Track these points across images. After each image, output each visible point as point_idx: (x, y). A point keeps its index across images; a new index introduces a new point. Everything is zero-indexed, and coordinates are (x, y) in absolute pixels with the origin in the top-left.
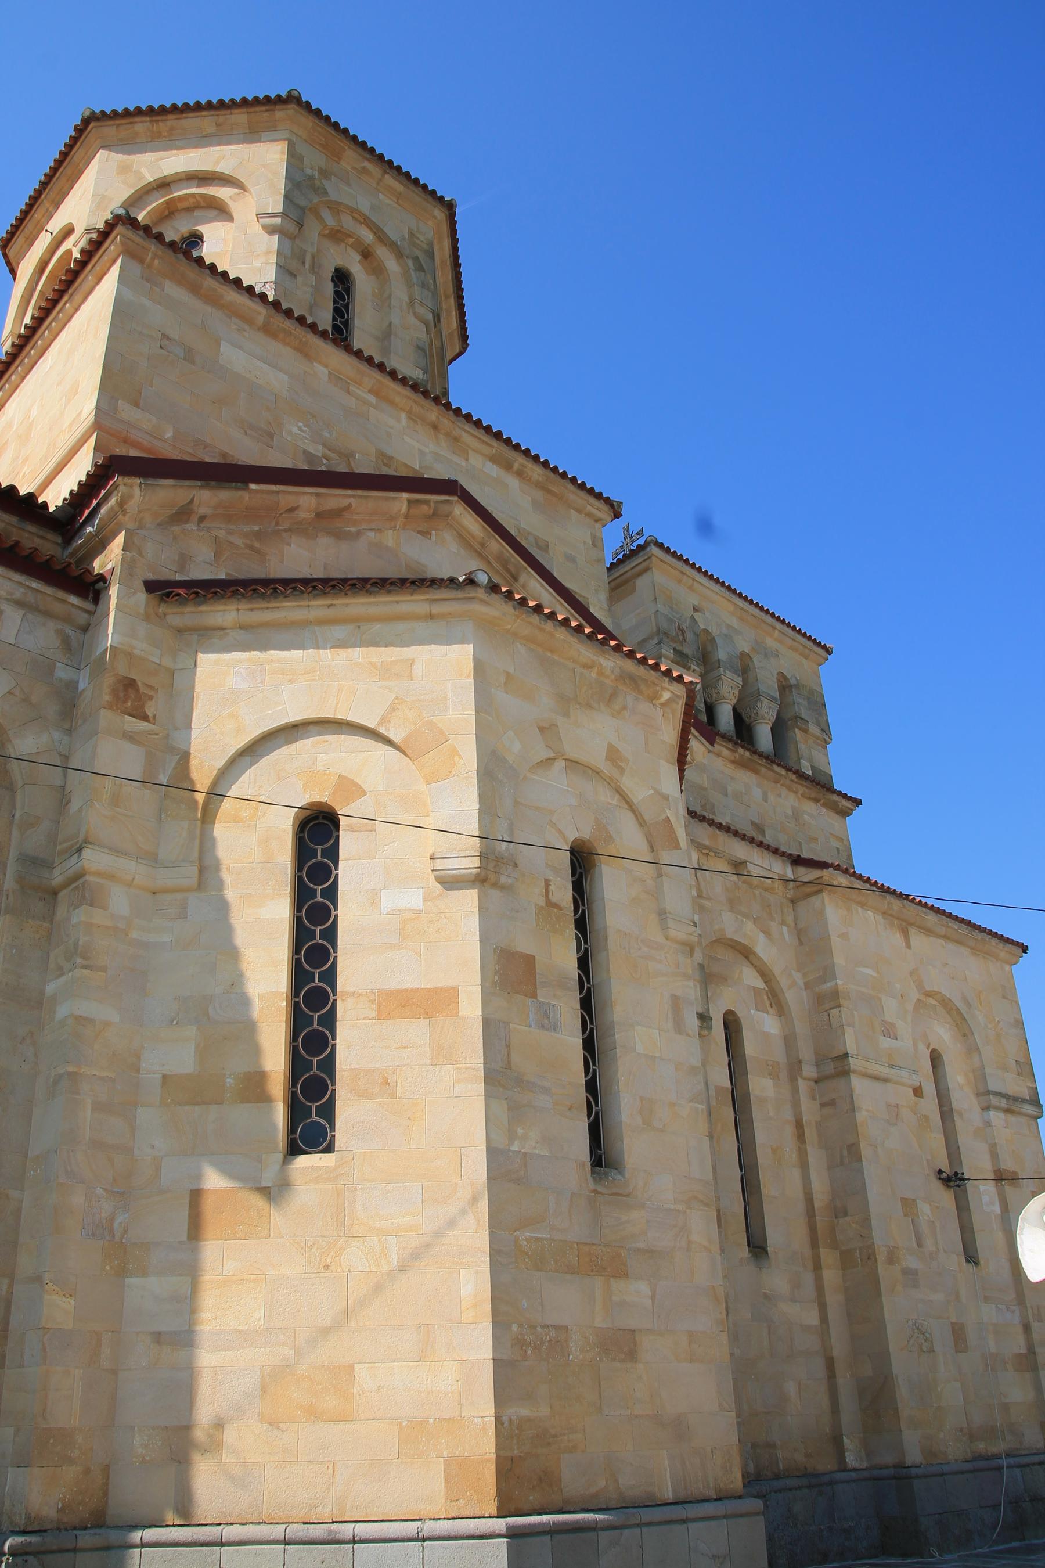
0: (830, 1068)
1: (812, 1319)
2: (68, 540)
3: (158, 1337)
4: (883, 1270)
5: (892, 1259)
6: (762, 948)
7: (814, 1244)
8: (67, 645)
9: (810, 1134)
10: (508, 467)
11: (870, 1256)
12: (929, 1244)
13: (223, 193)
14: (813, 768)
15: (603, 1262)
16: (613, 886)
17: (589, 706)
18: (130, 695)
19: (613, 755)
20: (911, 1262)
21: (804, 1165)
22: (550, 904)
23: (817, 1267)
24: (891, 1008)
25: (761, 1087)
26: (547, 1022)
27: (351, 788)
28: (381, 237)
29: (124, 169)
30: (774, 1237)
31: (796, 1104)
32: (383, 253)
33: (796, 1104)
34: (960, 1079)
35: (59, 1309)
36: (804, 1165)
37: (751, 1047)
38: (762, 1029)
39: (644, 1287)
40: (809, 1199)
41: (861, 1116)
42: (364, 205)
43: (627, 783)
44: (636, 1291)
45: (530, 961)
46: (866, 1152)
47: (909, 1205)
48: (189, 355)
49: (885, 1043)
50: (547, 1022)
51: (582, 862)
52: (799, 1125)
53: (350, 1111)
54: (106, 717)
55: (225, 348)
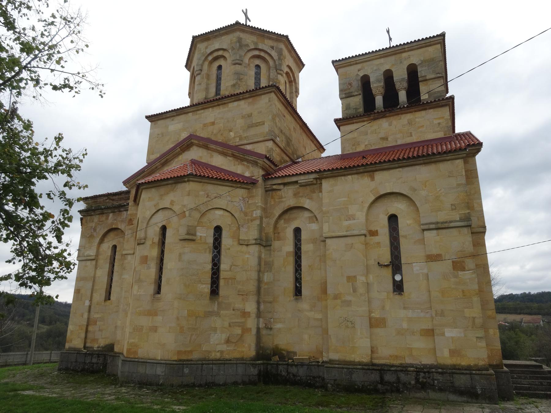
17: (168, 193)
19: (172, 203)
20: (348, 298)
22: (153, 243)
24: (353, 209)
28: (224, 50)
37: (304, 236)
39: (161, 318)
44: (159, 318)
45: (147, 257)
47: (351, 279)
49: (346, 223)
50: (149, 268)
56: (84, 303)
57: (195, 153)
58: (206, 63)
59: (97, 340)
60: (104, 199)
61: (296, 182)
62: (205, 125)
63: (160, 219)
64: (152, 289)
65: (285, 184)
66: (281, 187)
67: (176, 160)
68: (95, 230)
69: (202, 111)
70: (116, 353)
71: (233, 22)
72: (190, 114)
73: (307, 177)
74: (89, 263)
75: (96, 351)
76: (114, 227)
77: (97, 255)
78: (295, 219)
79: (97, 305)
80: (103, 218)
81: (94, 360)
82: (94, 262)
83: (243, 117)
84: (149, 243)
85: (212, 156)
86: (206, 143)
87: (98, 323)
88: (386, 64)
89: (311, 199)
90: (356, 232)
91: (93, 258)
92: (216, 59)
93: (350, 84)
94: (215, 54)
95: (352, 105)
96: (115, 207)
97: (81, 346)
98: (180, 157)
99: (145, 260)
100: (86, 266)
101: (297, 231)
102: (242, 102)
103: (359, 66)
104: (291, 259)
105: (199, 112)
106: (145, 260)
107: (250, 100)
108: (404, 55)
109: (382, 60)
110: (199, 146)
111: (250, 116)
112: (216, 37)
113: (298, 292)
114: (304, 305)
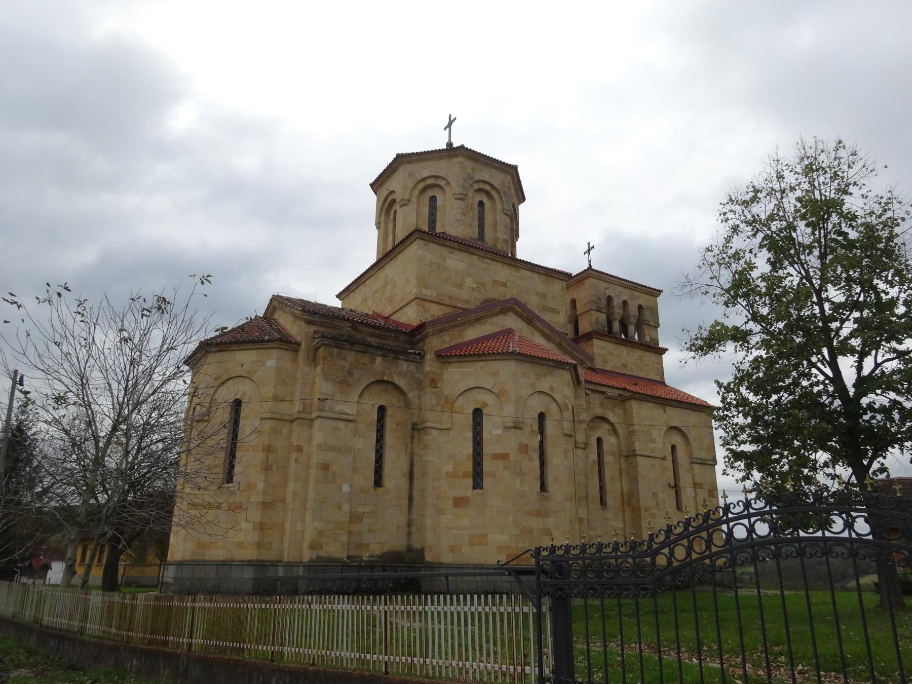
0: (631, 453)
1: (621, 525)
3: (448, 528)
4: (642, 512)
5: (647, 510)
6: (611, 417)
7: (623, 505)
8: (417, 369)
9: (624, 473)
10: (534, 271)
11: (639, 509)
12: (662, 506)
13: (442, 183)
14: (651, 339)
15: (542, 513)
16: (549, 424)
18: (434, 383)
19: (551, 388)
20: (655, 511)
21: (621, 482)
23: (624, 511)
24: (655, 434)
25: (608, 459)
26: (531, 460)
27: (485, 404)
29: (411, 174)
30: (610, 502)
31: (620, 464)
32: (493, 193)
33: (620, 464)
34: (683, 454)
35: (428, 522)
36: (621, 482)
37: (606, 447)
38: (610, 442)
40: (622, 492)
41: (639, 468)
42: (487, 178)
43: (554, 395)
44: (551, 520)
45: (527, 445)
46: (640, 478)
47: (655, 495)
48: (438, 266)
49: (651, 445)
50: (531, 460)
51: (542, 417)
52: (621, 470)
53: (486, 481)
54: (428, 390)
55: (448, 260)
56: (341, 488)
57: (510, 321)
59: (367, 546)
60: (347, 324)
61: (603, 393)
62: (495, 282)
63: (537, 404)
65: (593, 391)
66: (589, 392)
68: (350, 374)
70: (428, 563)
71: (512, 163)
72: (475, 257)
73: (614, 391)
74: (341, 425)
75: (368, 561)
76: (386, 378)
78: (598, 428)
79: (361, 491)
80: (365, 359)
81: (377, 574)
82: (351, 425)
83: (537, 294)
84: (527, 429)
85: (533, 335)
86: (530, 318)
87: (365, 520)
88: (625, 295)
89: (613, 412)
90: (657, 455)
92: (488, 194)
93: (600, 299)
94: (482, 186)
95: (600, 320)
96: (391, 351)
97: (343, 555)
99: (524, 449)
100: (336, 429)
101: (599, 440)
102: (535, 276)
103: (606, 285)
104: (596, 467)
105: (486, 260)
106: (524, 449)
107: (544, 278)
108: (636, 293)
109: (621, 289)
111: (544, 296)
112: (486, 164)
113: (603, 502)
114: (609, 515)
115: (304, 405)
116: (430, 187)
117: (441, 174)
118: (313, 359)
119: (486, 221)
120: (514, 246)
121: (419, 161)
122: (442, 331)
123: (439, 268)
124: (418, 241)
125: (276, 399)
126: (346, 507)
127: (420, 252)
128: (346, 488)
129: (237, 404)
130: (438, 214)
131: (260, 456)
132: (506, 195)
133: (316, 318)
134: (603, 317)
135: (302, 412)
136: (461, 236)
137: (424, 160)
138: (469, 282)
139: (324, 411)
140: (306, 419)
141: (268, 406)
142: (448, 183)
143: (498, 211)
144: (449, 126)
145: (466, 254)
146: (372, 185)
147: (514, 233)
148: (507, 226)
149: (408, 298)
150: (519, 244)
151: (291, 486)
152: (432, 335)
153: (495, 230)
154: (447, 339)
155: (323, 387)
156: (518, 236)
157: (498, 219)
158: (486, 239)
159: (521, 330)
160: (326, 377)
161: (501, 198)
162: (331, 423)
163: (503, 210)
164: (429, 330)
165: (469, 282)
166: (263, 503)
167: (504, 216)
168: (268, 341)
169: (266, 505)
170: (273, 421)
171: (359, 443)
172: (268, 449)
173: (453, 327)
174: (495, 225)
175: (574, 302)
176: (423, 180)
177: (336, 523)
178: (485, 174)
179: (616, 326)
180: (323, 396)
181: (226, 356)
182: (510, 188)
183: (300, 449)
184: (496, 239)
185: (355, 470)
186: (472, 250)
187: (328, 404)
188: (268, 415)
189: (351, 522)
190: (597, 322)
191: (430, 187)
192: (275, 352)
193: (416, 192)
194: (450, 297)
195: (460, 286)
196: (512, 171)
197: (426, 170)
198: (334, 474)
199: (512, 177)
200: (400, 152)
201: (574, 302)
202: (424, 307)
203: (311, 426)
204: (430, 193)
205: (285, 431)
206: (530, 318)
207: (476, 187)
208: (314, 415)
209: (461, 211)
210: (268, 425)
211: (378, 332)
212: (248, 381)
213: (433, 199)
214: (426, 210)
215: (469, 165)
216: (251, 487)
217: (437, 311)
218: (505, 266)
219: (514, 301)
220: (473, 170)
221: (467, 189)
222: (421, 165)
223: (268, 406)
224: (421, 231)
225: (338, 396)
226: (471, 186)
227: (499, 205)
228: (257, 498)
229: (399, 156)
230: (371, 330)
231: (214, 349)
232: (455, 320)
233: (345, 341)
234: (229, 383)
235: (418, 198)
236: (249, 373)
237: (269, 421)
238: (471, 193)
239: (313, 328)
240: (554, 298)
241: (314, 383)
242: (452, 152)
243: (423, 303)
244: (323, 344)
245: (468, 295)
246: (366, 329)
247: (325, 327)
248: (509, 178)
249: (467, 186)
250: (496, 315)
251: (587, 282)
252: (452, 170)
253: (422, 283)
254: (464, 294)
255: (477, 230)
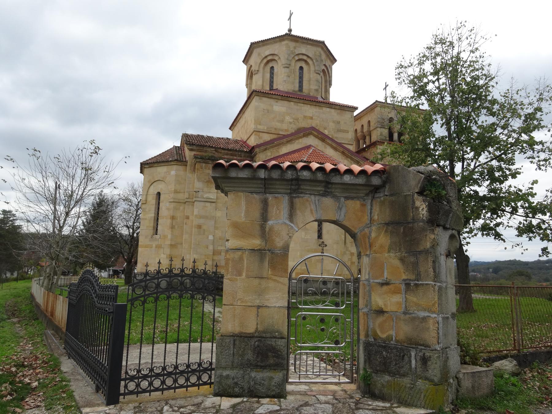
2: (252, 153)
13: (276, 58)
28: (308, 57)
29: (259, 54)
42: (304, 51)
48: (268, 111)
56: (208, 237)
58: (294, 61)
60: (212, 149)
62: (305, 117)
64: (316, 235)
67: (297, 141)
69: (302, 105)
72: (292, 103)
74: (208, 204)
77: (217, 198)
79: (220, 239)
82: (214, 204)
83: (334, 122)
85: (326, 148)
86: (323, 138)
91: (213, 201)
92: (306, 61)
95: (384, 133)
98: (300, 140)
100: (205, 207)
102: (333, 110)
105: (299, 104)
107: (339, 111)
110: (316, 137)
111: (339, 123)
115: (189, 195)
116: (269, 61)
117: (276, 53)
118: (194, 170)
119: (304, 79)
120: (327, 92)
121: (263, 45)
122: (266, 149)
123: (268, 112)
124: (256, 97)
125: (176, 192)
126: (211, 247)
127: (257, 104)
128: (211, 237)
129: (159, 194)
130: (275, 77)
131: (169, 221)
132: (317, 61)
133: (194, 147)
134: (386, 132)
135: (189, 198)
136: (286, 90)
137: (266, 45)
138: (288, 119)
139: (198, 197)
140: (189, 202)
141: (172, 195)
142: (280, 58)
143: (311, 72)
144: (290, 19)
145: (286, 102)
146: (243, 61)
147: (328, 83)
148: (317, 81)
149: (252, 131)
150: (332, 90)
151: (185, 237)
152: (260, 152)
153: (310, 84)
154: (269, 154)
155: (198, 185)
156: (330, 84)
157: (311, 76)
158: (304, 90)
159: (317, 146)
160: (199, 180)
161: (314, 63)
162: (203, 204)
163: (315, 71)
164: (257, 150)
165: (288, 119)
166: (171, 245)
167: (315, 74)
168: (171, 161)
169: (172, 246)
170: (175, 204)
171: (219, 214)
172: (173, 218)
173: (273, 147)
174: (309, 81)
175: (369, 122)
176: (266, 57)
177: (205, 255)
178: (303, 49)
179: (396, 136)
180: (197, 190)
181: (152, 170)
182: (320, 56)
183: (188, 218)
184: (310, 90)
185: (216, 228)
186: (290, 99)
187: (200, 194)
188: (172, 200)
189: (213, 254)
190: (381, 134)
191: (269, 61)
192: (175, 167)
193: (262, 65)
194: (275, 129)
195: (282, 121)
196: (321, 44)
197: (267, 51)
198: (204, 230)
199: (322, 48)
200: (253, 41)
201: (369, 122)
202: (259, 136)
203: (193, 205)
204: (271, 65)
205: (181, 208)
206: (323, 138)
207: (297, 58)
208: (194, 199)
209: (286, 74)
210: (173, 205)
211: (229, 152)
212: (163, 182)
213: (272, 68)
214: (268, 75)
215: (292, 44)
216: (165, 237)
217: (267, 138)
218: (312, 107)
219: (313, 128)
220: (295, 48)
221: (291, 61)
222: (265, 47)
223: (172, 195)
224: (256, 91)
225: (206, 189)
226: (293, 58)
227: (312, 68)
228: (168, 242)
229: (252, 44)
230: (226, 151)
231: (147, 166)
232: (273, 143)
233: (209, 159)
234: (155, 184)
235: (264, 68)
236: (163, 178)
237: (173, 203)
238: (293, 63)
239: (193, 153)
240: (345, 123)
241: (194, 183)
242: (289, 37)
243: (258, 133)
244: (197, 162)
245: (287, 126)
246: (223, 151)
247: (200, 152)
248: (320, 49)
249: (291, 58)
250: (301, 138)
251: (376, 109)
252: (281, 49)
253: (258, 122)
254: (285, 126)
255: (298, 85)
